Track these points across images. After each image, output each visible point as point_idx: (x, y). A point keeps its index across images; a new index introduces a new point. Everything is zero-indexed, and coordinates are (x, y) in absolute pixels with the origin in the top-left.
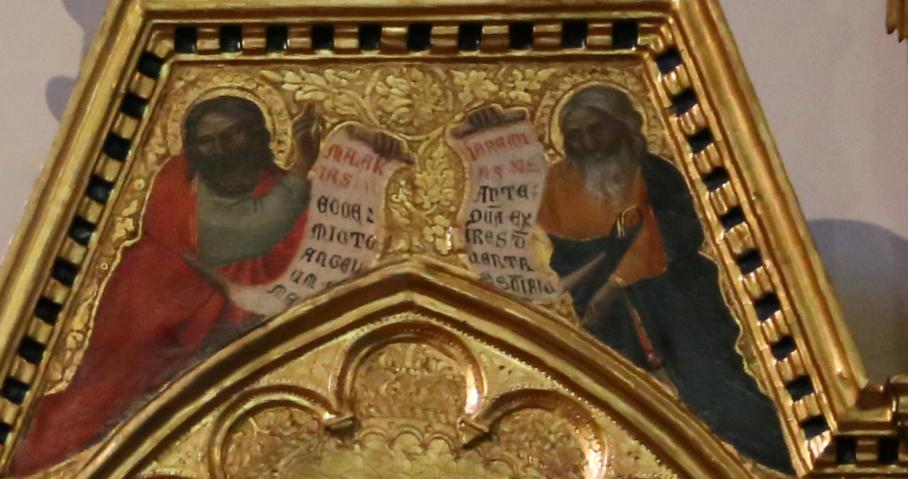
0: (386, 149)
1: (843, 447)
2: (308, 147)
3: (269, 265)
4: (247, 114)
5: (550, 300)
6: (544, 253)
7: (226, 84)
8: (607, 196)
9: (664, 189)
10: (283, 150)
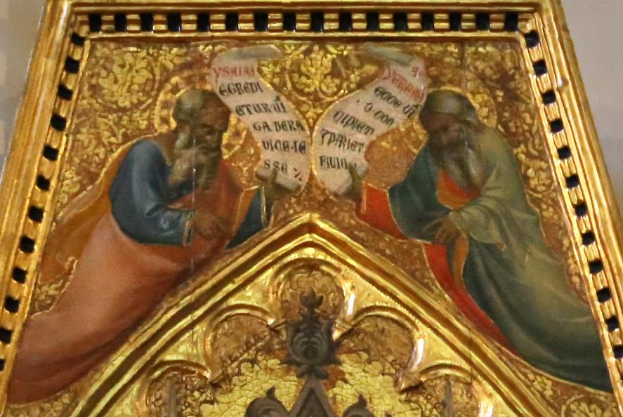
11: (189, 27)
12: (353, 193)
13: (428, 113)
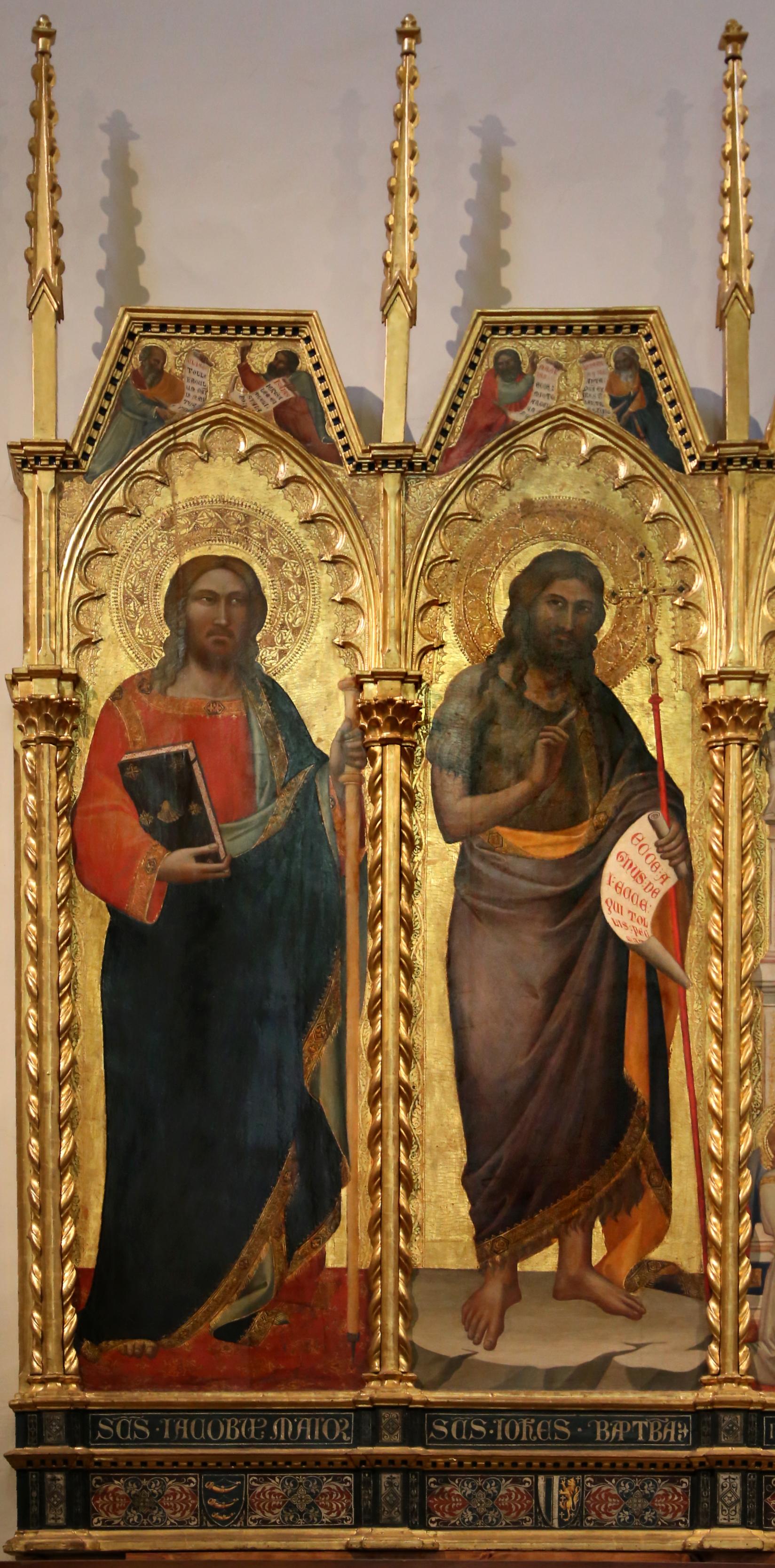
0: (558, 367)
1: (701, 465)
2: (533, 366)
3: (520, 404)
4: (514, 355)
5: (610, 417)
6: (607, 401)
7: (508, 345)
8: (628, 382)
9: (645, 380)
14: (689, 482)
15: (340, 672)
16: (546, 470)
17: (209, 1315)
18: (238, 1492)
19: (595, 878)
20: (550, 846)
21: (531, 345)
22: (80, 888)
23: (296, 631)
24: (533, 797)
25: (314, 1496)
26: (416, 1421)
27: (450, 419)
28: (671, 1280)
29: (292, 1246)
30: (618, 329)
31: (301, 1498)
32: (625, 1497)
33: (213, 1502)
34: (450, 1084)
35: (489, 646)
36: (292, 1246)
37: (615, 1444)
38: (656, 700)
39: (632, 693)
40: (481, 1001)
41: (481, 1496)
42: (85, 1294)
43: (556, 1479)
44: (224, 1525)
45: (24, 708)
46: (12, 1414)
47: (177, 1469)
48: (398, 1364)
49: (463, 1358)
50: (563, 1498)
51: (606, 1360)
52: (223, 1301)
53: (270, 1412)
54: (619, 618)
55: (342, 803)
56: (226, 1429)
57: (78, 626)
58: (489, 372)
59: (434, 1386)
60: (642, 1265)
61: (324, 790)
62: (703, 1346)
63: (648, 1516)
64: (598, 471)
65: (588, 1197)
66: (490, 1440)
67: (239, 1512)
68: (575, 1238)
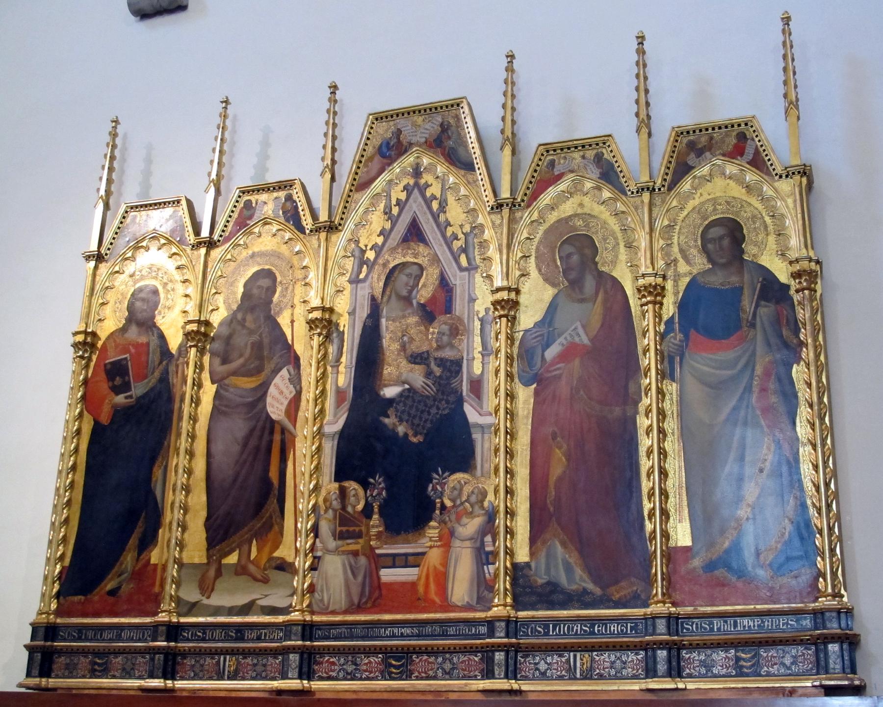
1: (311, 231)
4: (250, 201)
5: (282, 220)
6: (281, 212)
10: (254, 205)
11: (395, 117)
12: (426, 142)
13: (442, 125)
14: (308, 238)
15: (181, 322)
16: (260, 240)
17: (106, 586)
18: (106, 663)
19: (265, 394)
20: (248, 383)
21: (256, 197)
22: (85, 412)
23: (169, 308)
24: (243, 365)
25: (134, 664)
26: (173, 631)
27: (226, 226)
28: (284, 566)
29: (139, 555)
30: (285, 187)
31: (128, 666)
32: (255, 665)
33: (96, 667)
34: (203, 485)
35: (235, 307)
36: (139, 555)
37: (252, 640)
38: (292, 322)
39: (284, 320)
40: (219, 447)
41: (198, 665)
42: (64, 576)
43: (228, 657)
44: (99, 677)
45: (75, 345)
46: (30, 629)
47: (84, 652)
48: (170, 605)
49: (197, 602)
50: (230, 666)
51: (252, 603)
52: (112, 579)
53: (120, 627)
54: (282, 292)
55: (177, 373)
56: (105, 635)
57: (98, 314)
58: (242, 208)
59: (186, 615)
60: (271, 559)
61: (172, 368)
62: (292, 595)
63: (264, 674)
64: (278, 239)
65: (250, 531)
66: (204, 640)
67: (105, 671)
68: (246, 547)
